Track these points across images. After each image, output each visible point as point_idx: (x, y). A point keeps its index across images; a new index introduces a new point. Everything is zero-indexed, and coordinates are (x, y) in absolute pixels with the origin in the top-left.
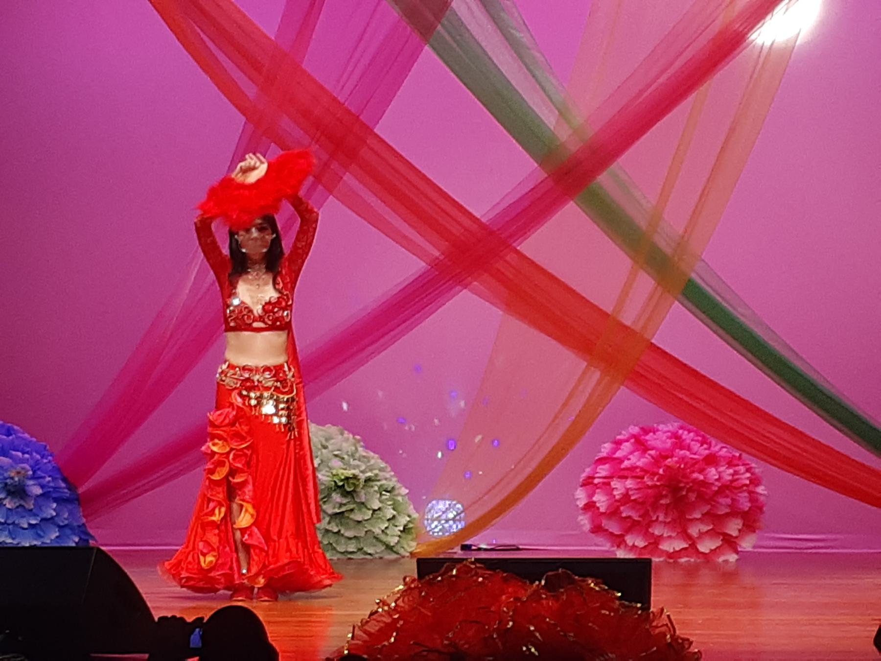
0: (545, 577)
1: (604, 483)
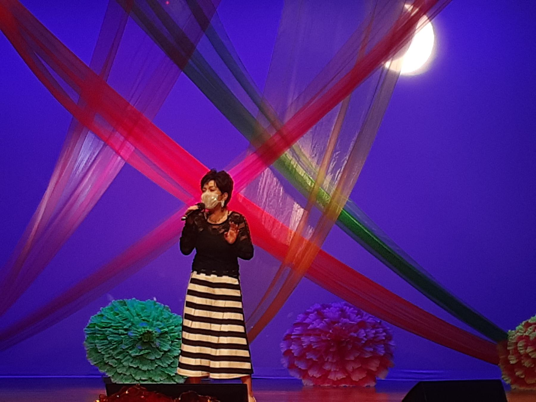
0: (181, 395)
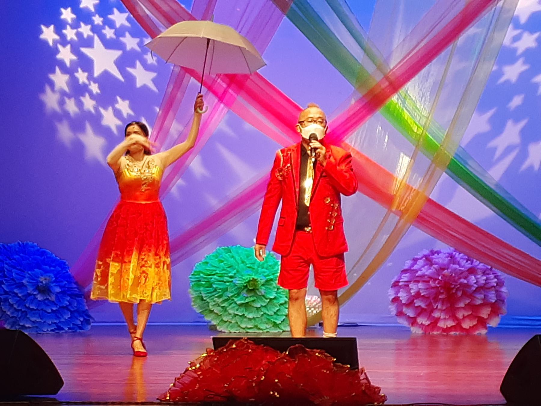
1: (405, 285)
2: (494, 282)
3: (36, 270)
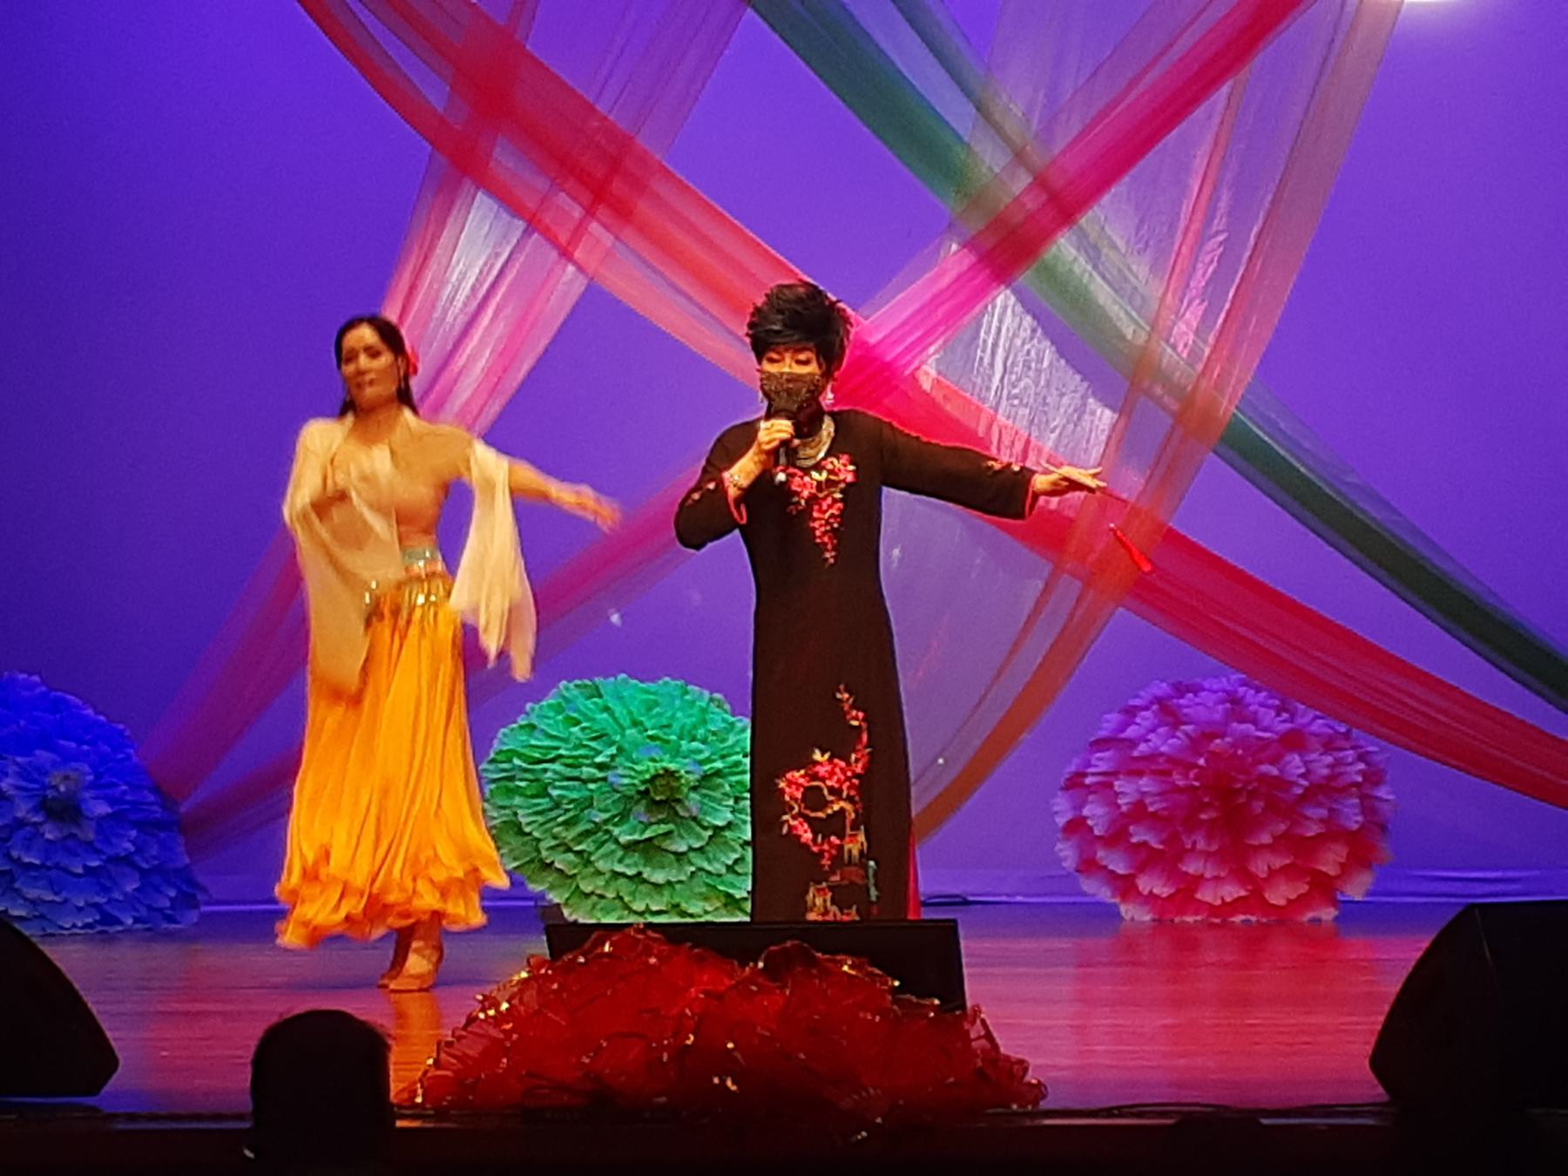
0: (763, 956)
2: (1356, 771)
3: (38, 752)
